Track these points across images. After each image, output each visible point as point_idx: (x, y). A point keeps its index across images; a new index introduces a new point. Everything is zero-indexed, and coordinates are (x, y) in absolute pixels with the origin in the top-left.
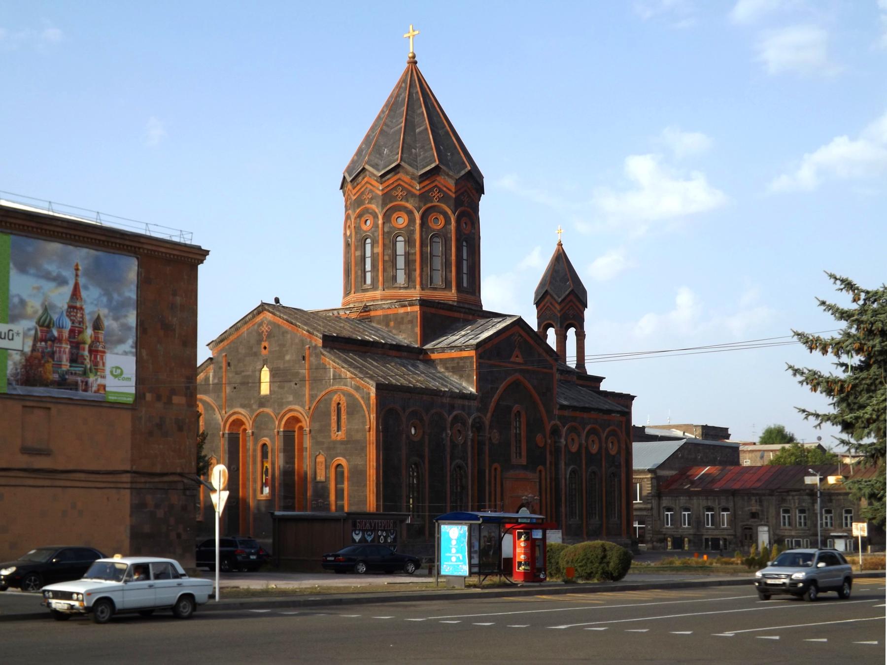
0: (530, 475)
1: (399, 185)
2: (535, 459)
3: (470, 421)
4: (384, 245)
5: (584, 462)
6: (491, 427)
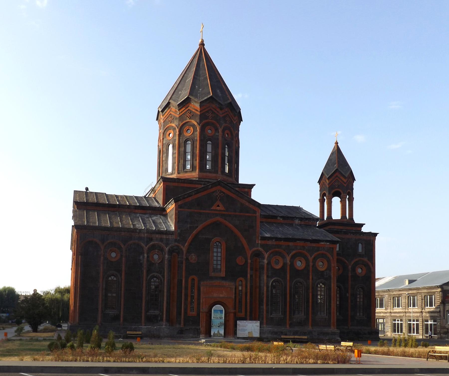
0: (227, 283)
2: (233, 272)
3: (167, 249)
5: (288, 276)
6: (189, 252)
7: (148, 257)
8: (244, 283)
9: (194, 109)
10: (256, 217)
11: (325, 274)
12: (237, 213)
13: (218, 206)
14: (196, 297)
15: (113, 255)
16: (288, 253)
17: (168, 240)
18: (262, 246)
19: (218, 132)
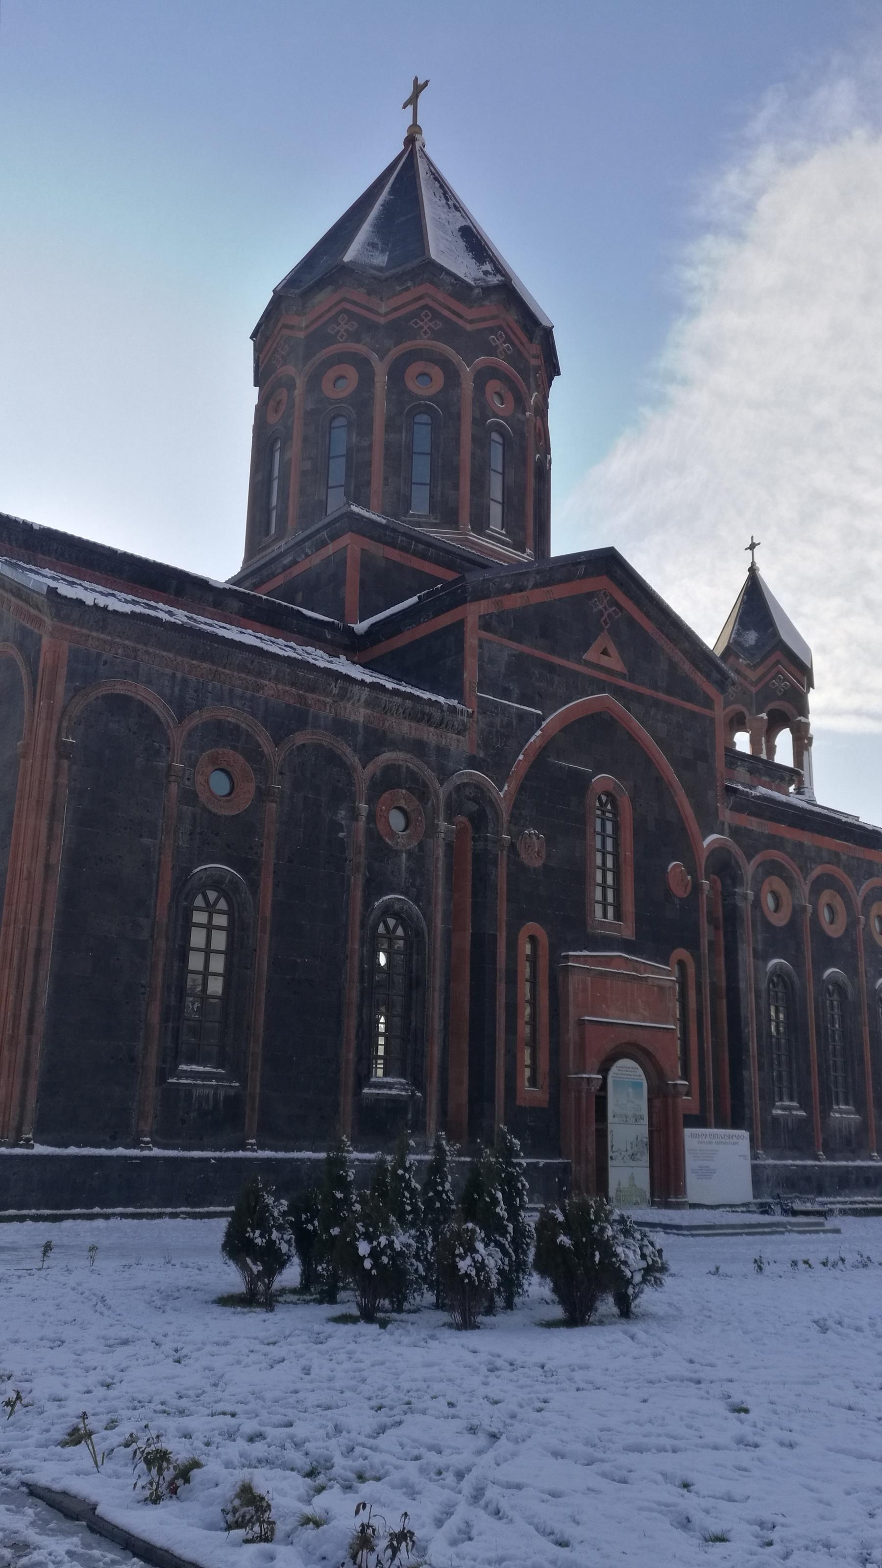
1: (345, 311)
4: (305, 439)
6: (514, 818)
7: (371, 817)
8: (691, 970)
9: (449, 309)
10: (712, 720)
12: (662, 696)
13: (605, 652)
14: (544, 1019)
15: (219, 784)
17: (443, 752)
18: (736, 833)
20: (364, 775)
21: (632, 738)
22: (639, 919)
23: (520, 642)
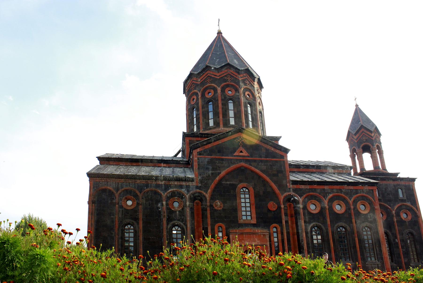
0: (259, 230)
5: (328, 220)
6: (213, 198)
7: (167, 204)
8: (279, 229)
9: (213, 75)
11: (369, 217)
12: (263, 159)
13: (241, 152)
16: (324, 197)
18: (295, 190)
19: (239, 92)
20: (164, 195)
21: (252, 171)
22: (257, 218)
23: (211, 155)
